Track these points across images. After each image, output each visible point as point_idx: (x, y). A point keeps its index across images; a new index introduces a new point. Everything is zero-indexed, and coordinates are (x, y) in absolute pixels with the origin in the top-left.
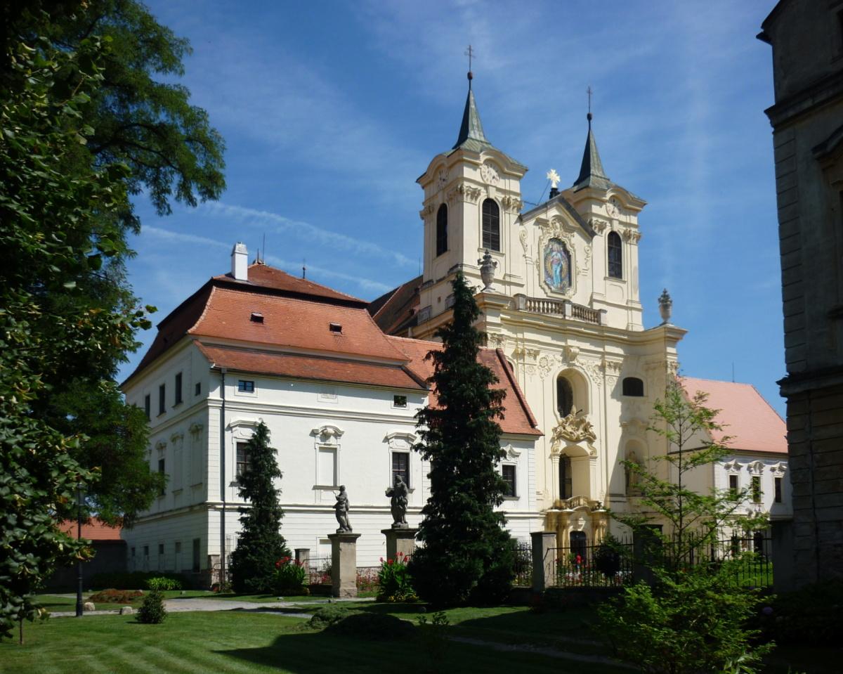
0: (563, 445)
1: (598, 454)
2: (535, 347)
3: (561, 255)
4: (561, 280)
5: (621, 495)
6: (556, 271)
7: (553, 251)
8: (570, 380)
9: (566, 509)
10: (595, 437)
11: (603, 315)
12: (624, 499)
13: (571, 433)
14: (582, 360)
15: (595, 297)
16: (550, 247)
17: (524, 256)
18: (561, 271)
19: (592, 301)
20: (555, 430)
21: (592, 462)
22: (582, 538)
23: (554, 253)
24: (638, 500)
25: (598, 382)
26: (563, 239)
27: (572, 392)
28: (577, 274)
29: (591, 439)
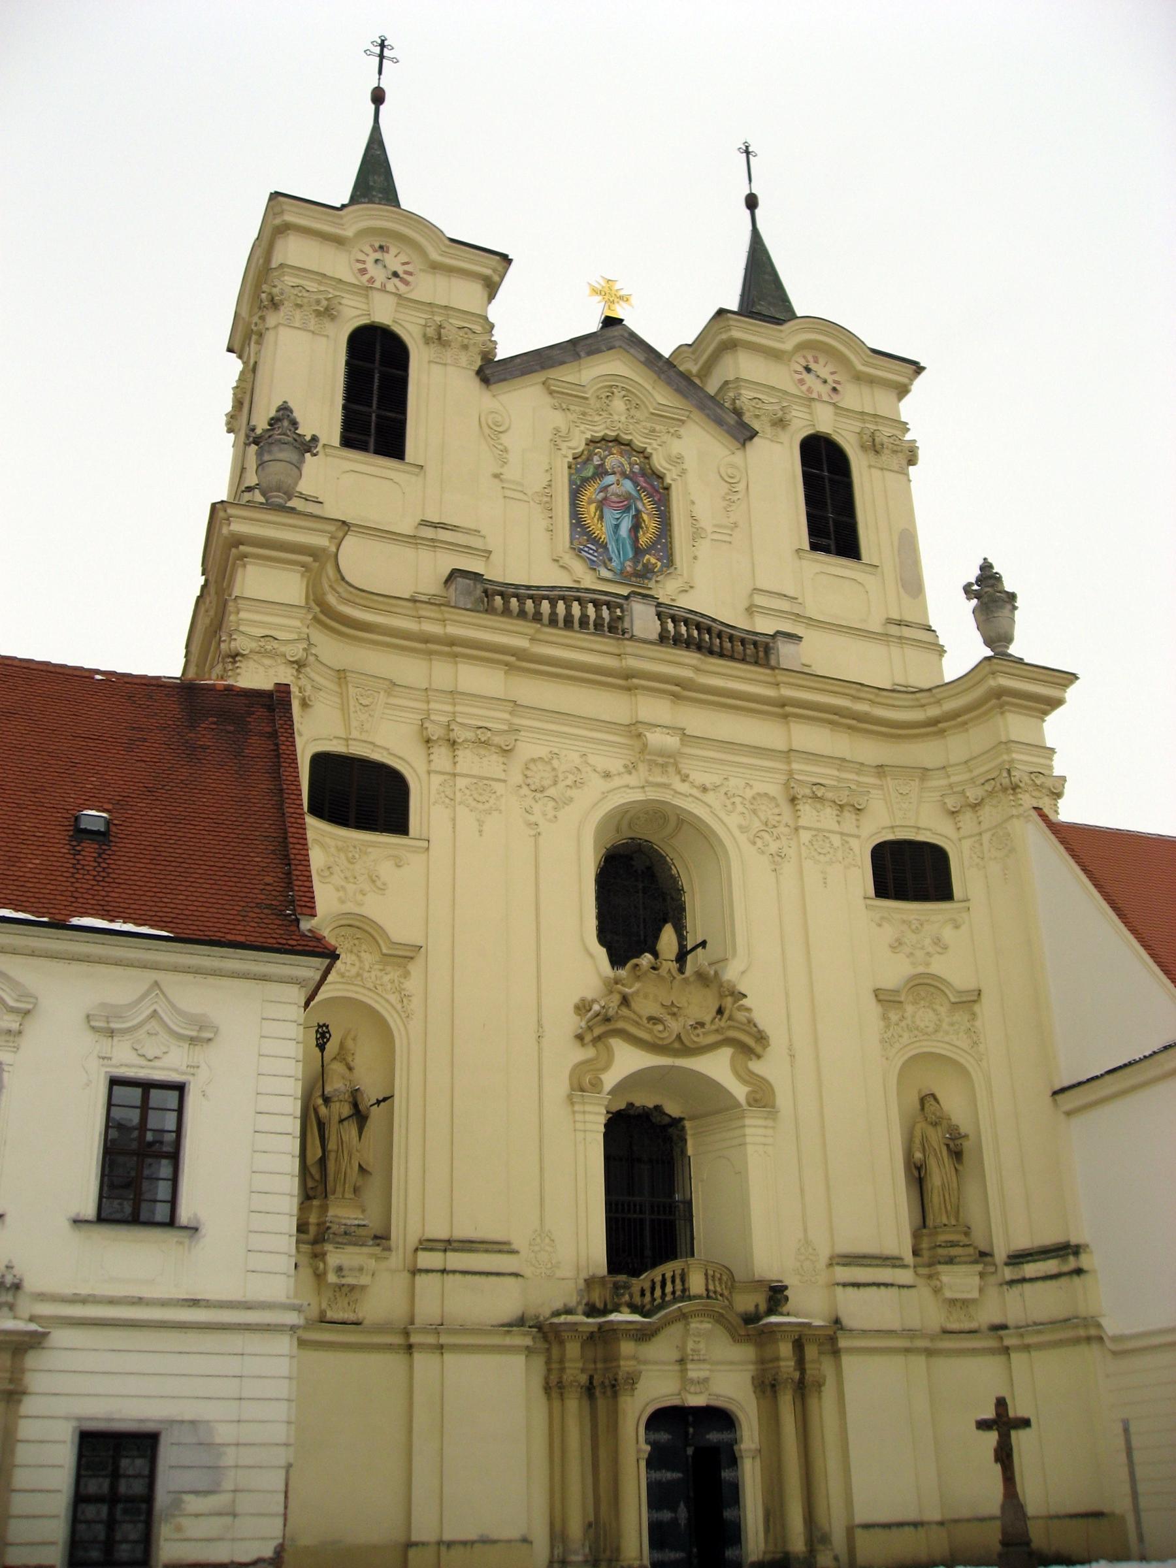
0: (628, 1061)
1: (783, 1100)
2: (497, 719)
3: (636, 484)
4: (638, 552)
5: (892, 1261)
6: (617, 527)
7: (607, 473)
8: (668, 850)
9: (616, 1309)
10: (762, 1038)
11: (785, 649)
12: (904, 1276)
13: (653, 1019)
14: (698, 777)
15: (759, 600)
16: (596, 461)
17: (497, 476)
18: (636, 527)
19: (751, 610)
20: (582, 1007)
21: (754, 1128)
22: (714, 1437)
23: (610, 479)
24: (960, 1280)
25: (773, 847)
26: (639, 441)
27: (680, 891)
28: (697, 534)
29: (749, 1044)
